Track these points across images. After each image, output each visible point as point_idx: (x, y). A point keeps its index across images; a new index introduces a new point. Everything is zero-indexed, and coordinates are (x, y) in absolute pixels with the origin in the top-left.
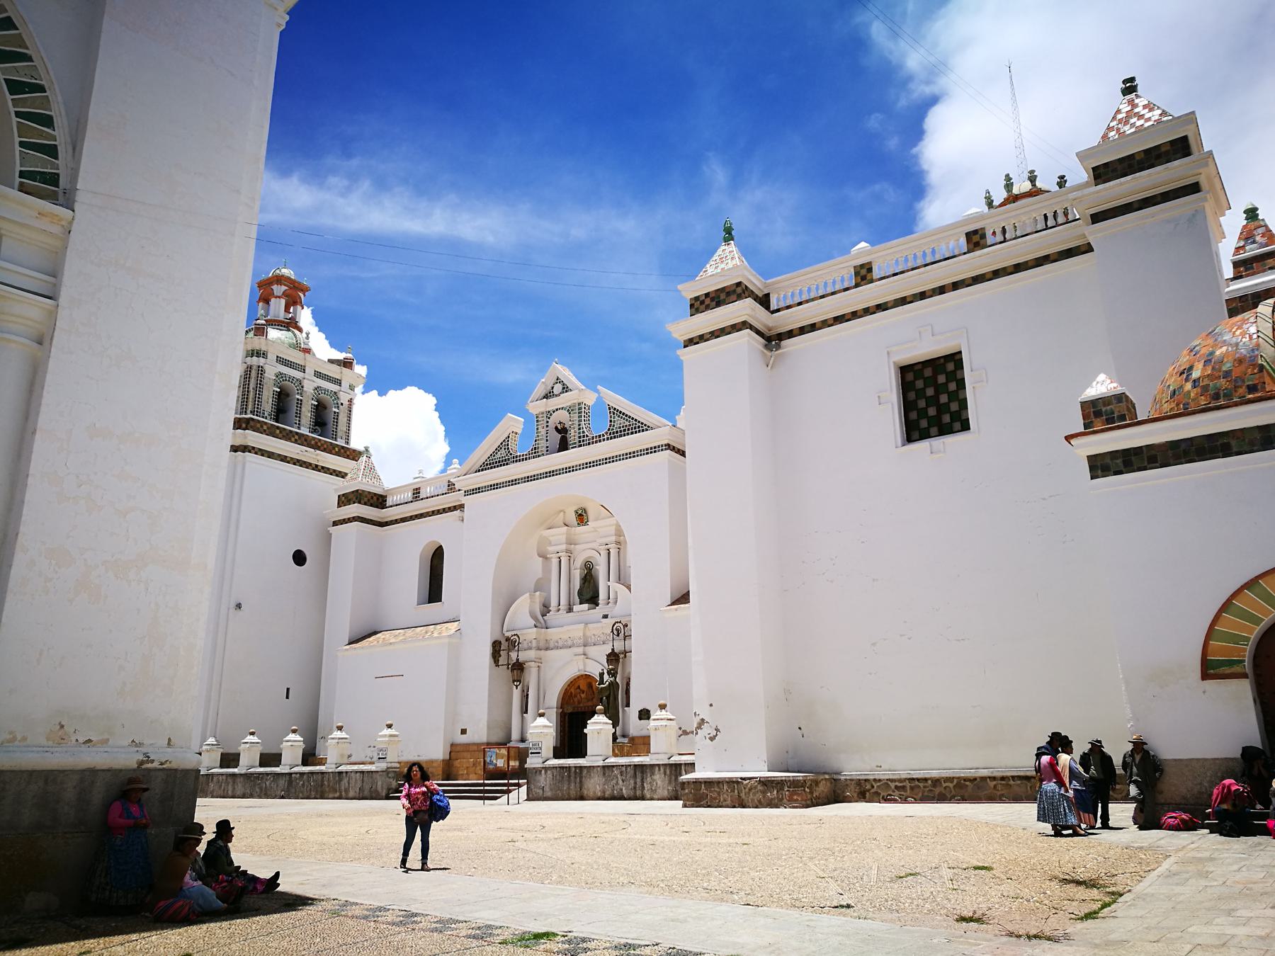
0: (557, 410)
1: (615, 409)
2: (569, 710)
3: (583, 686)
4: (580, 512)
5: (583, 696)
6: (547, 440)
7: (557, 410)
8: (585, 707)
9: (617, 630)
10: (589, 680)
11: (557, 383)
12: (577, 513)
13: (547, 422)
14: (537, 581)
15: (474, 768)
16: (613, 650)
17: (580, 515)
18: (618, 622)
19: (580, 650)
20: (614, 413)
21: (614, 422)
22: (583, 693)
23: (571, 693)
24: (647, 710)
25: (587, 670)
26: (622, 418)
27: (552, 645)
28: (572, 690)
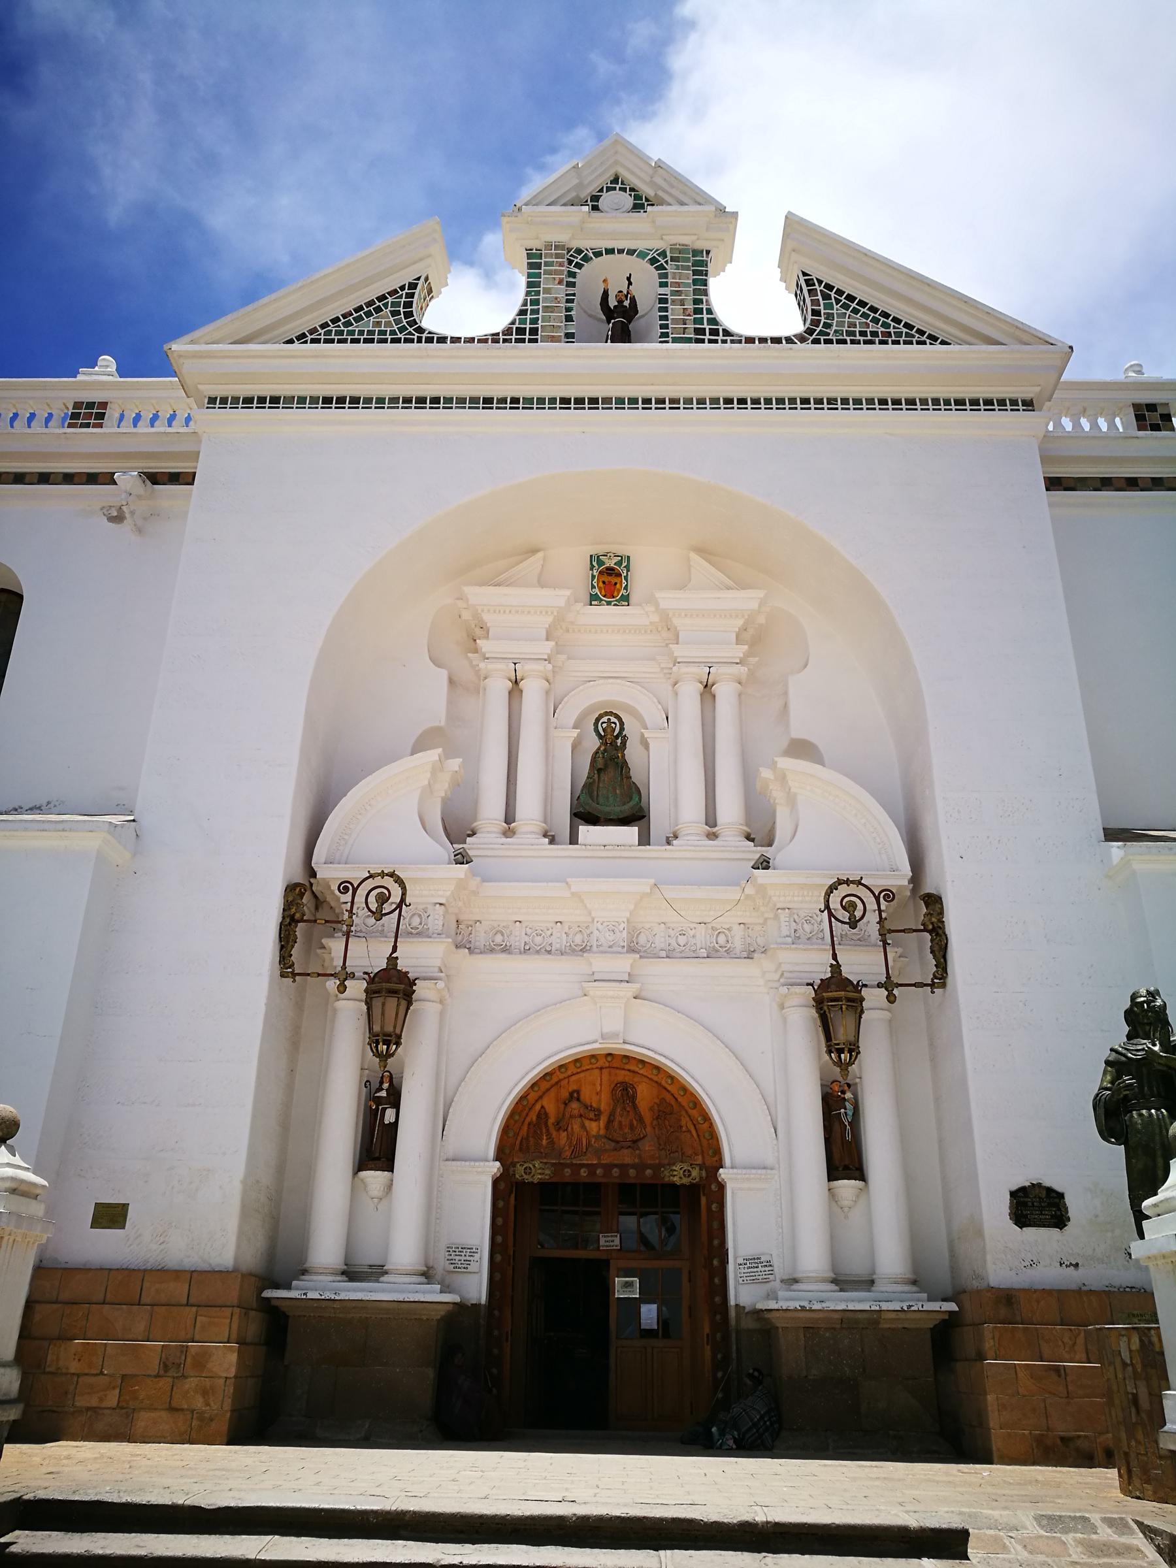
0: (610, 251)
1: (829, 287)
2: (537, 1171)
3: (597, 1090)
4: (611, 563)
5: (594, 1127)
6: (569, 319)
7: (610, 251)
8: (608, 1168)
9: (849, 907)
10: (622, 1076)
11: (609, 189)
12: (600, 563)
13: (572, 275)
14: (421, 735)
15: (165, 1383)
16: (836, 968)
17: (610, 571)
18: (848, 882)
19: (622, 964)
20: (826, 297)
21: (829, 316)
22: (597, 1118)
23: (543, 1115)
24: (1050, 1190)
25: (629, 1039)
26: (855, 311)
27: (481, 937)
28: (549, 1104)
